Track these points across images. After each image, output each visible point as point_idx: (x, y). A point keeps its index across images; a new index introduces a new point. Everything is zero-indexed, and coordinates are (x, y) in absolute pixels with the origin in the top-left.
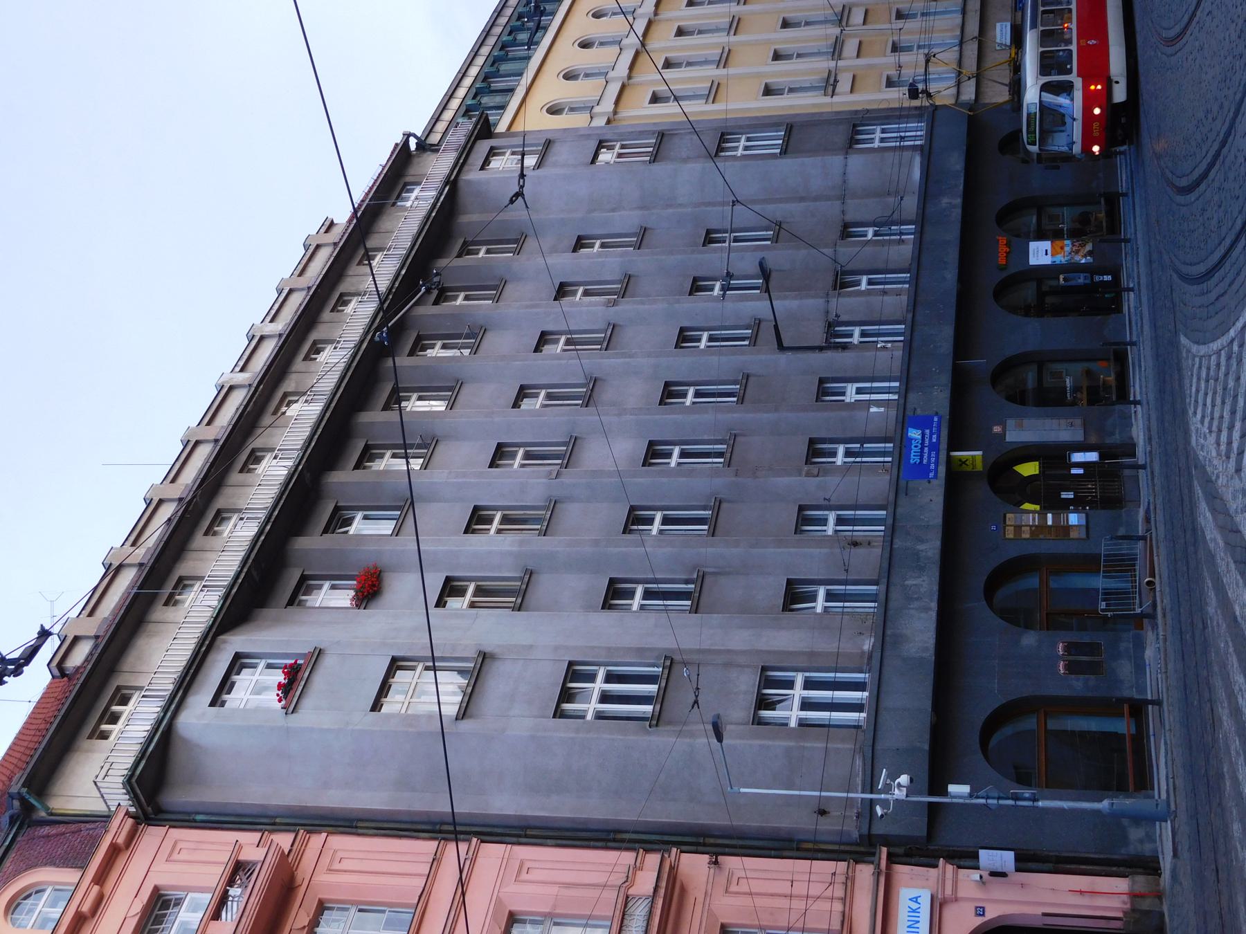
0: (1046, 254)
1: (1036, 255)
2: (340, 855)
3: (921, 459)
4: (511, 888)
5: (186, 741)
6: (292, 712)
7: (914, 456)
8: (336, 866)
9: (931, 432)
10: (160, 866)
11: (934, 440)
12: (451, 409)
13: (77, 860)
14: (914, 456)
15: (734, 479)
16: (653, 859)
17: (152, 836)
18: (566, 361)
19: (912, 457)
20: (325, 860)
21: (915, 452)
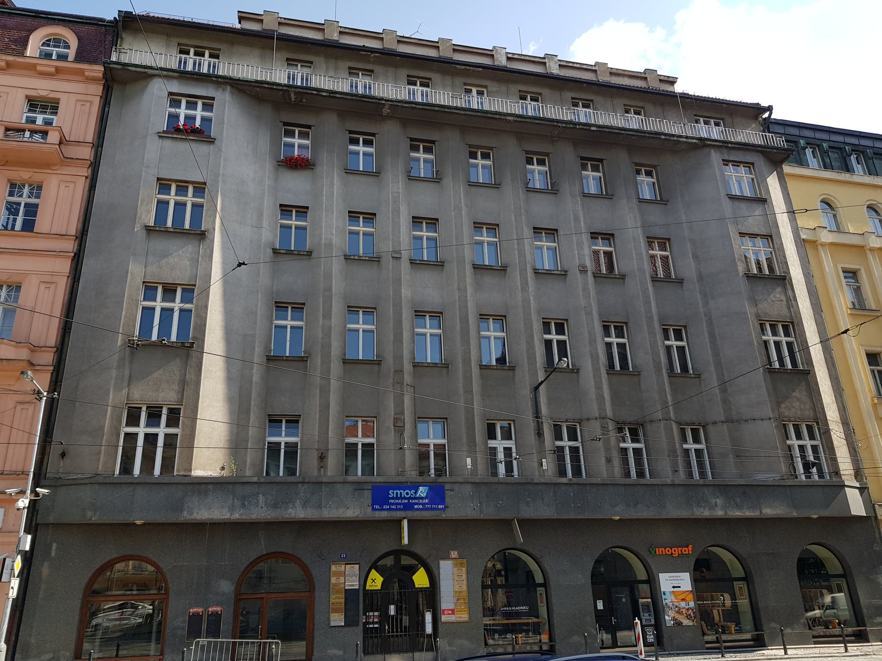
0: (674, 587)
1: (671, 578)
2: (71, 186)
3: (393, 498)
4: (34, 280)
5: (146, 86)
6: (729, 197)
7: (397, 493)
8: (63, 185)
9: (426, 504)
10: (73, 98)
11: (416, 507)
12: (583, 196)
13: (81, 57)
14: (397, 493)
15: (392, 370)
16: (48, 358)
17: (98, 89)
18: (516, 248)
19: (395, 492)
20: (68, 178)
21: (401, 493)
